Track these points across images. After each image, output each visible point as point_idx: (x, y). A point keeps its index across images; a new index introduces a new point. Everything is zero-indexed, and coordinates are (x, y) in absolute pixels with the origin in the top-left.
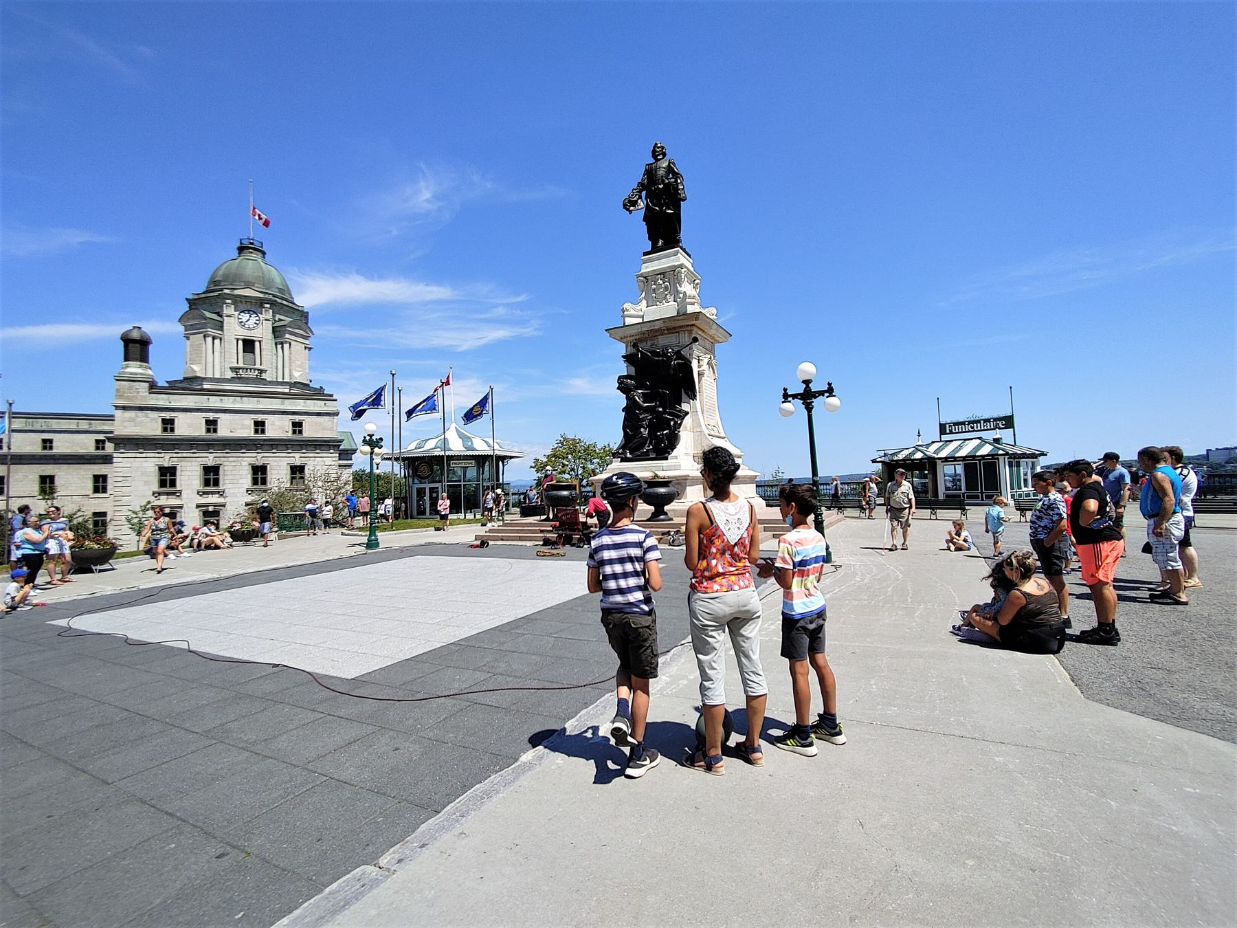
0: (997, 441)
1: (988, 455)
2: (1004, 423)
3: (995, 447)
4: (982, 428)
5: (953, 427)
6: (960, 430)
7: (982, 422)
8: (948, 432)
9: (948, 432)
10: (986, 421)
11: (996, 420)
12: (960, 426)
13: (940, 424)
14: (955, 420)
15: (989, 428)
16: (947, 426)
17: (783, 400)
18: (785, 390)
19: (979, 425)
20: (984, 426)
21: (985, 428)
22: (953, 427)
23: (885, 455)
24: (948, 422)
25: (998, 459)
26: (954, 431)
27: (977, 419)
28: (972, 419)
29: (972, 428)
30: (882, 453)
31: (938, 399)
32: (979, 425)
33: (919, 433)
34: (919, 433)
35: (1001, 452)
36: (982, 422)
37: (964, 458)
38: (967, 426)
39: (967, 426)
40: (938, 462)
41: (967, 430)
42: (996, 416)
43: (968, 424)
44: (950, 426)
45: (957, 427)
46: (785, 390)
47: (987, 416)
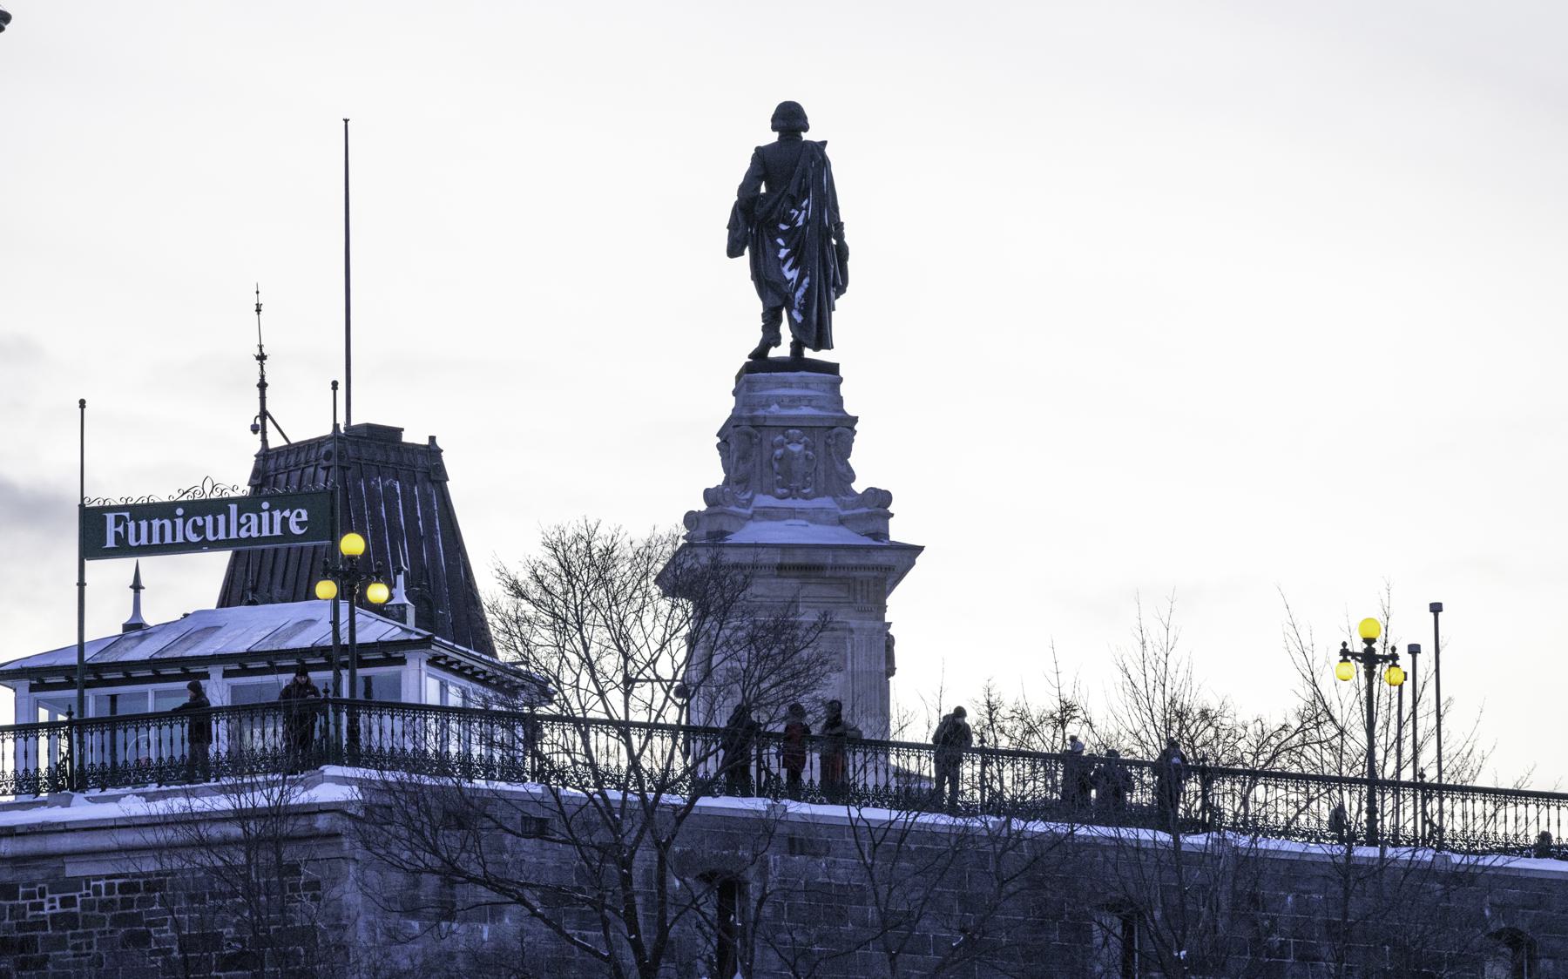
2: (304, 518)
4: (233, 535)
5: (132, 525)
6: (156, 541)
7: (233, 508)
8: (111, 542)
9: (111, 542)
12: (156, 523)
15: (254, 534)
16: (111, 517)
17: (1341, 658)
18: (1344, 644)
19: (221, 518)
20: (240, 526)
21: (243, 534)
22: (132, 525)
24: (116, 500)
26: (132, 542)
27: (215, 495)
29: (199, 530)
32: (221, 518)
36: (233, 508)
38: (179, 522)
39: (179, 522)
41: (180, 539)
43: (186, 518)
44: (118, 520)
45: (144, 524)
46: (1344, 644)
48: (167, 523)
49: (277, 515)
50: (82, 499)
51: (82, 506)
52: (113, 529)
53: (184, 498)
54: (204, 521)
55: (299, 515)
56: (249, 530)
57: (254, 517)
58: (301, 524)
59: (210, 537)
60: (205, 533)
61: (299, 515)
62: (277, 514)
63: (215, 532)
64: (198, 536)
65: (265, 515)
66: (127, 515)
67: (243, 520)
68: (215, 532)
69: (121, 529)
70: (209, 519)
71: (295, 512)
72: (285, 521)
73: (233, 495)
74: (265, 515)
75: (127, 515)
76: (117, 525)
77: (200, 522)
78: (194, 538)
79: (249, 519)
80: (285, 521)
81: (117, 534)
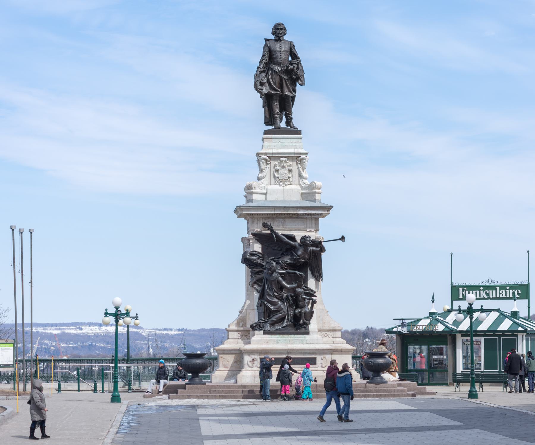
0: (514, 314)
1: (508, 331)
2: (520, 292)
3: (514, 322)
4: (498, 296)
7: (498, 288)
8: (461, 297)
9: (461, 297)
10: (503, 287)
11: (512, 287)
13: (453, 287)
14: (469, 283)
15: (504, 296)
16: (461, 289)
19: (494, 291)
20: (500, 294)
21: (501, 296)
23: (403, 325)
24: (462, 284)
25: (517, 336)
27: (492, 284)
28: (487, 284)
29: (488, 294)
30: (399, 323)
31: (451, 254)
32: (494, 291)
33: (433, 298)
34: (433, 298)
35: (520, 329)
36: (498, 288)
37: (484, 333)
39: (482, 292)
40: (459, 336)
41: (482, 297)
42: (511, 283)
44: (463, 290)
47: (503, 282)
48: (478, 292)
49: (511, 291)
50: (452, 283)
51: (451, 285)
52: (462, 293)
53: (482, 284)
54: (489, 292)
55: (518, 291)
56: (502, 295)
57: (504, 291)
58: (518, 294)
59: (491, 297)
60: (489, 295)
61: (518, 291)
62: (511, 291)
63: (492, 295)
64: (487, 296)
65: (508, 291)
66: (466, 288)
67: (501, 292)
68: (492, 295)
69: (464, 293)
70: (491, 291)
71: (517, 290)
72: (514, 293)
73: (497, 284)
74: (508, 291)
75: (466, 288)
76: (463, 291)
77: (488, 292)
78: (486, 297)
79: (502, 291)
80: (514, 293)
81: (463, 294)
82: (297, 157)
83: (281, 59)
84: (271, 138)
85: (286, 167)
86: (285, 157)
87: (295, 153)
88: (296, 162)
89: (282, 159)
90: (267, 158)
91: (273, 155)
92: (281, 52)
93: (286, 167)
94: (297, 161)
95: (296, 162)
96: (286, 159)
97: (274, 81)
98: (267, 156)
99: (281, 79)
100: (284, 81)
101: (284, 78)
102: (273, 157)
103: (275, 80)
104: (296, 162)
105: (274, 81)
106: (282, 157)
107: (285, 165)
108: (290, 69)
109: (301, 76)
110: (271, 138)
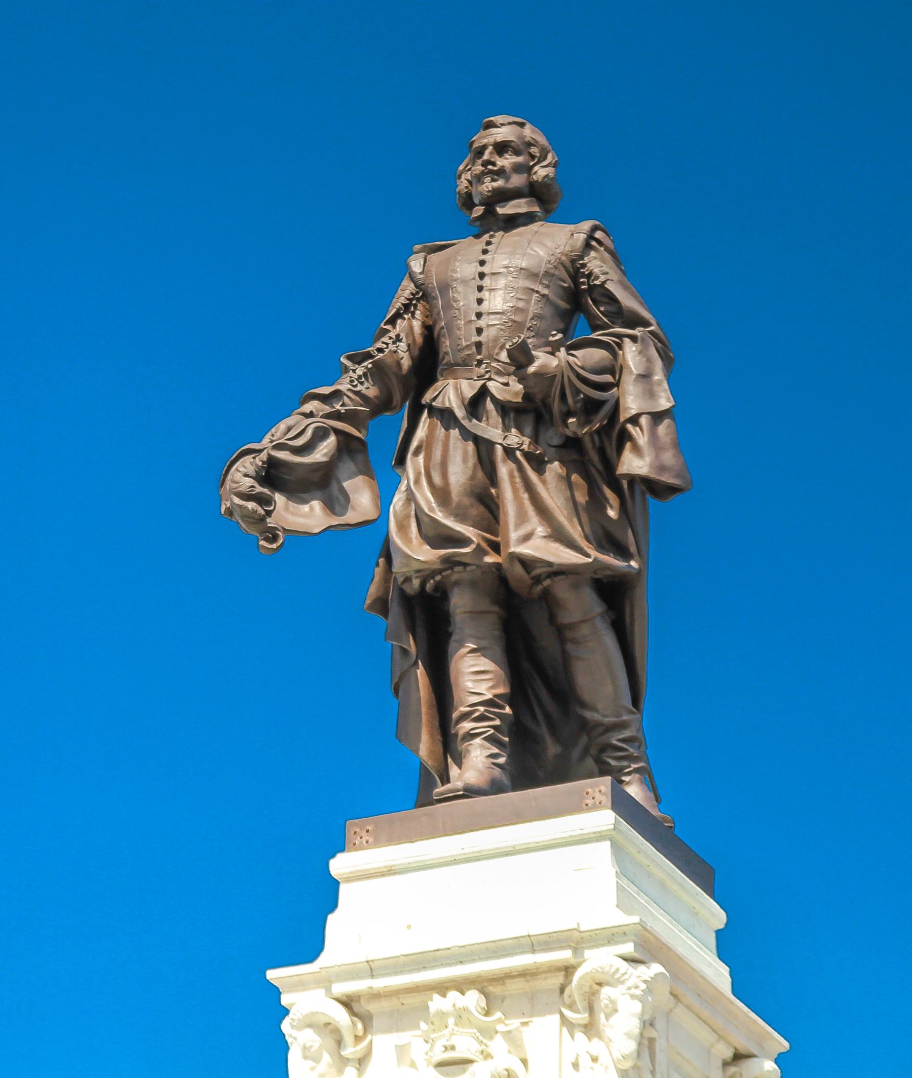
82: (559, 979)
83: (482, 323)
84: (390, 872)
85: (469, 1062)
86: (461, 985)
87: (533, 944)
88: (562, 1016)
89: (437, 1003)
90: (341, 1016)
91: (380, 983)
92: (486, 282)
93: (469, 1062)
94: (567, 1013)
95: (562, 1016)
96: (473, 999)
97: (437, 479)
98: (347, 1003)
99: (484, 448)
100: (504, 470)
101: (509, 452)
102: (385, 1005)
103: (445, 475)
104: (558, 1016)
105: (437, 479)
106: (442, 988)
107: (465, 1046)
108: (535, 374)
109: (634, 420)
110: (390, 872)
